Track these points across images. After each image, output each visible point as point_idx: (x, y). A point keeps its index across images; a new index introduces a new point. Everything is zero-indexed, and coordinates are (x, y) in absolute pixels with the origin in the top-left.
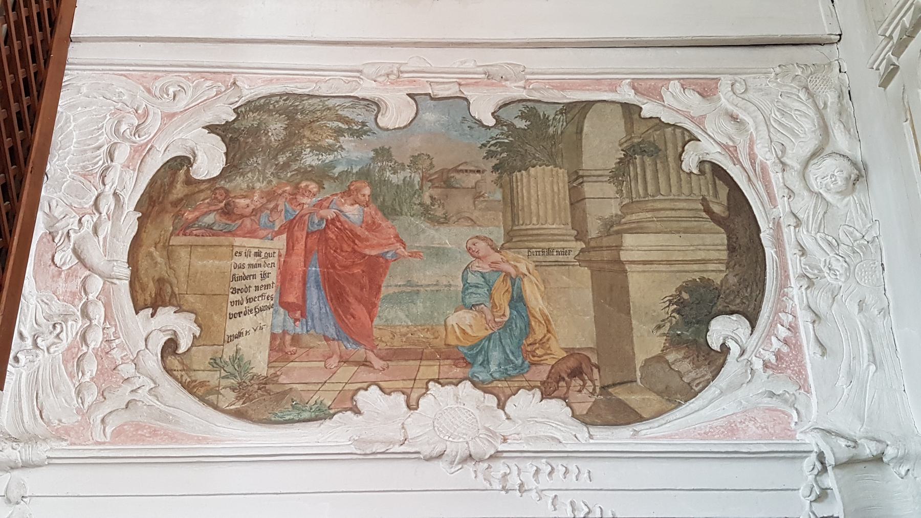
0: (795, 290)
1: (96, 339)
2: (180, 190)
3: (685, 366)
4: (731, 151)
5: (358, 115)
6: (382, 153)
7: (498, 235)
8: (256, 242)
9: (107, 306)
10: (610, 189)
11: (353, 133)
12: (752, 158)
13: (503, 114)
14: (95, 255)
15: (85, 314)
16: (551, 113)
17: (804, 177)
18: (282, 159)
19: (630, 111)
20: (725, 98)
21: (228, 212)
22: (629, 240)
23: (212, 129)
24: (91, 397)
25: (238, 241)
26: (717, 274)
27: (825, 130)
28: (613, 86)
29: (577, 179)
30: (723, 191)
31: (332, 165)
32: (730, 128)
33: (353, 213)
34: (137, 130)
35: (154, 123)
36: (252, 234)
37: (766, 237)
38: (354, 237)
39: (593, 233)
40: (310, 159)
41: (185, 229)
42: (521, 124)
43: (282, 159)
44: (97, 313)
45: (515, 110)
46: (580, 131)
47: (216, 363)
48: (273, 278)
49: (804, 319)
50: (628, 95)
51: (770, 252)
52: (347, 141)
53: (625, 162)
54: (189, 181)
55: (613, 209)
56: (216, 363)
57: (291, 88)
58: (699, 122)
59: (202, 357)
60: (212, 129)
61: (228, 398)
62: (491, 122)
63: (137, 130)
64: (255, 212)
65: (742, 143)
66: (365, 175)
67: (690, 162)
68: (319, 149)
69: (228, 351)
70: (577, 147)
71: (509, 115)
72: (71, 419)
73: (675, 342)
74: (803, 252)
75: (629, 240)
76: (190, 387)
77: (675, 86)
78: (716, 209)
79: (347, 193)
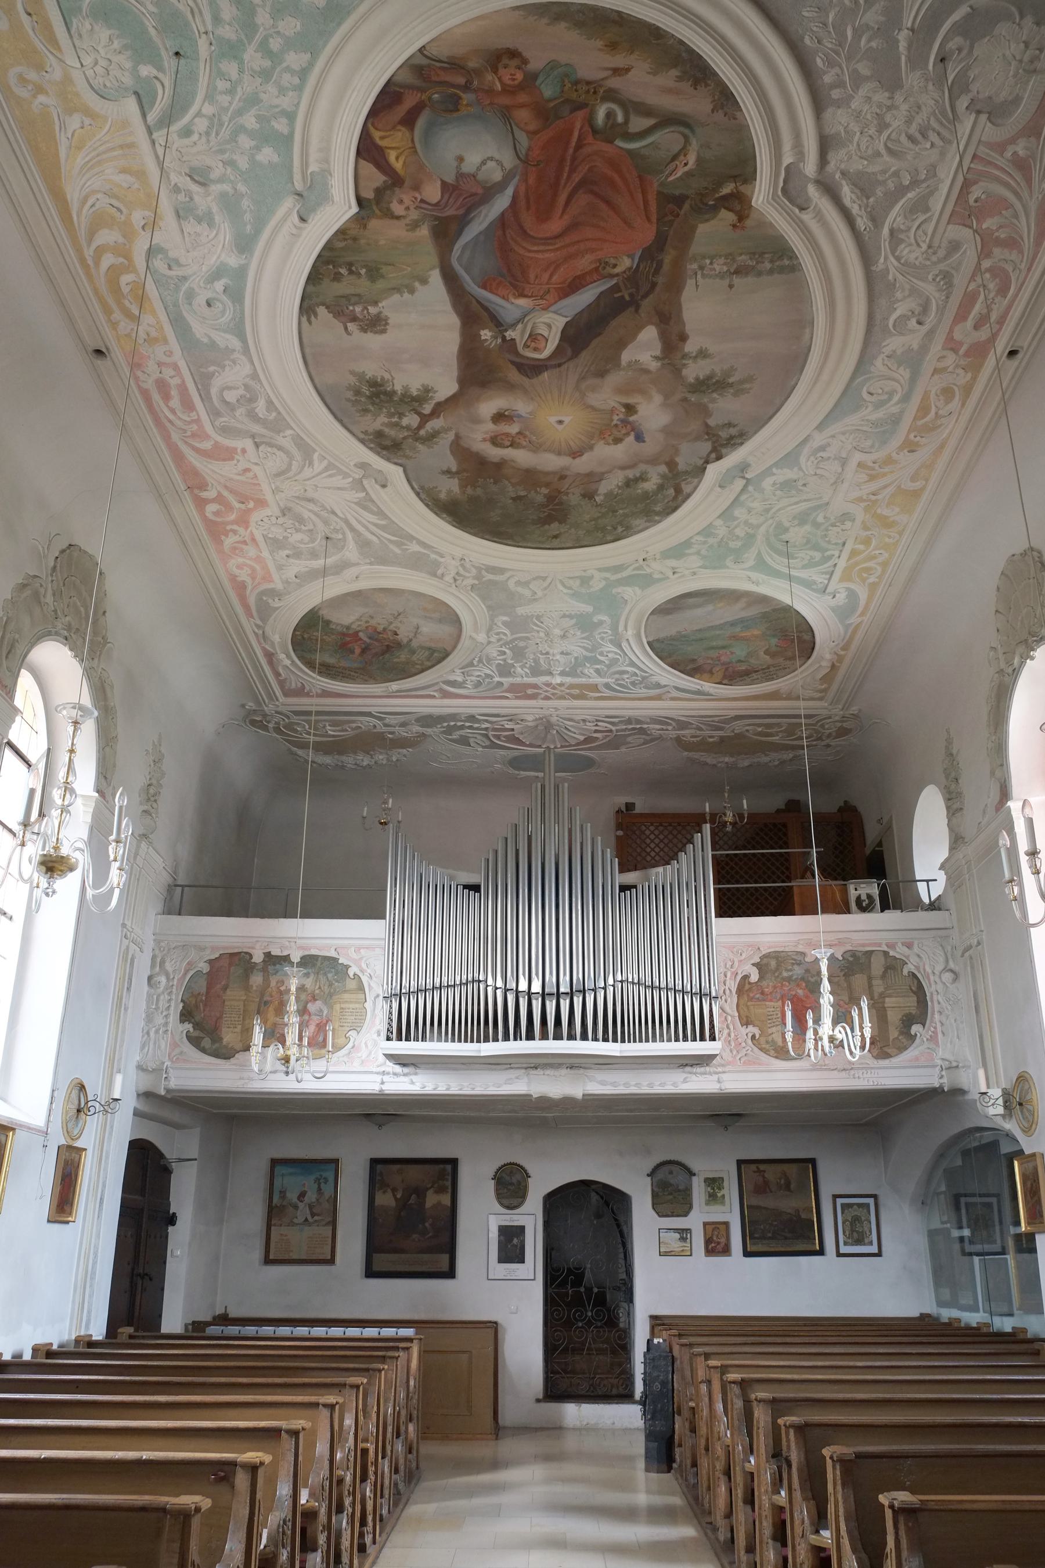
0: (937, 1016)
1: (732, 1035)
2: (747, 987)
3: (904, 1040)
4: (917, 968)
5: (799, 958)
6: (807, 971)
7: (846, 998)
8: (773, 1003)
9: (734, 1025)
10: (880, 982)
11: (799, 964)
12: (924, 970)
13: (845, 956)
14: (727, 1008)
15: (728, 1027)
16: (860, 954)
17: (940, 978)
18: (776, 974)
19: (886, 953)
20: (916, 949)
21: (762, 993)
22: (887, 1000)
23: (753, 965)
24: (735, 1052)
25: (767, 1003)
26: (914, 1011)
27: (947, 961)
28: (880, 945)
29: (870, 979)
30: (916, 982)
31: (792, 976)
32: (917, 959)
33: (800, 992)
34: (732, 967)
35: (736, 964)
36: (771, 1001)
37: (928, 998)
38: (802, 1001)
39: (876, 998)
40: (785, 974)
41: (751, 999)
42: (851, 959)
43: (776, 974)
44: (731, 1027)
45: (849, 954)
46: (870, 961)
47: (767, 1042)
48: (779, 1015)
49: (939, 1025)
50: (885, 949)
51: (929, 1003)
52: (796, 967)
53: (885, 972)
54: (750, 983)
55: (881, 989)
56: (767, 1042)
57: (777, 949)
58: (907, 957)
59: (763, 1040)
60: (753, 965)
61: (772, 1052)
62: (841, 958)
63: (732, 967)
64: (771, 993)
65: (921, 964)
66: (802, 979)
67: (905, 972)
68: (787, 970)
69: (770, 1038)
70: (869, 967)
71: (847, 956)
72: (730, 1059)
73: (901, 1033)
74: (939, 1003)
75: (887, 1000)
76: (761, 1049)
77: (900, 945)
78: (913, 988)
79: (798, 985)
